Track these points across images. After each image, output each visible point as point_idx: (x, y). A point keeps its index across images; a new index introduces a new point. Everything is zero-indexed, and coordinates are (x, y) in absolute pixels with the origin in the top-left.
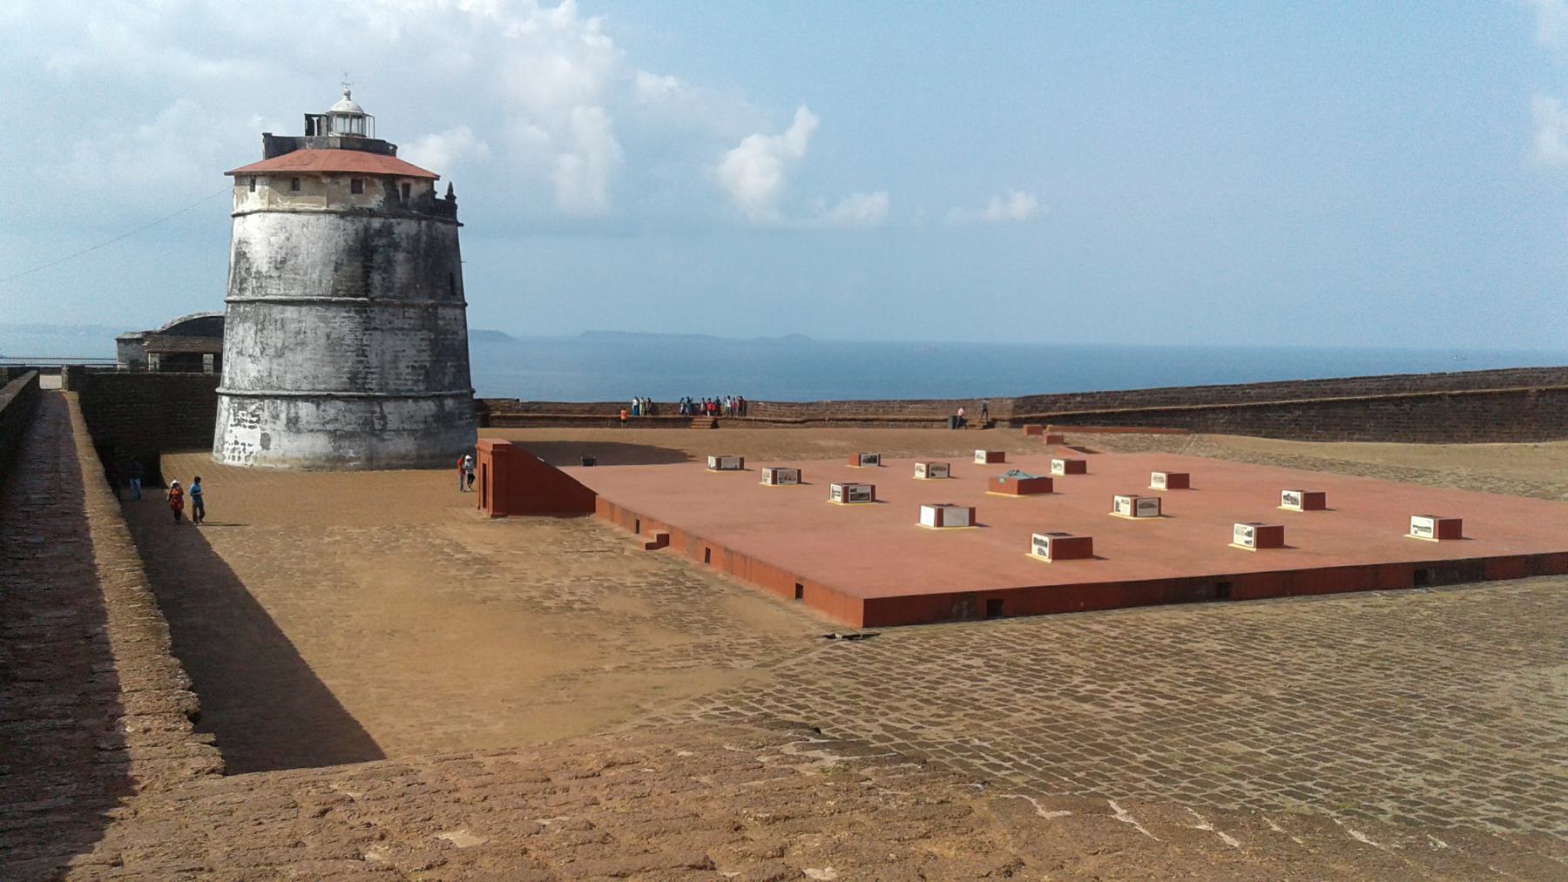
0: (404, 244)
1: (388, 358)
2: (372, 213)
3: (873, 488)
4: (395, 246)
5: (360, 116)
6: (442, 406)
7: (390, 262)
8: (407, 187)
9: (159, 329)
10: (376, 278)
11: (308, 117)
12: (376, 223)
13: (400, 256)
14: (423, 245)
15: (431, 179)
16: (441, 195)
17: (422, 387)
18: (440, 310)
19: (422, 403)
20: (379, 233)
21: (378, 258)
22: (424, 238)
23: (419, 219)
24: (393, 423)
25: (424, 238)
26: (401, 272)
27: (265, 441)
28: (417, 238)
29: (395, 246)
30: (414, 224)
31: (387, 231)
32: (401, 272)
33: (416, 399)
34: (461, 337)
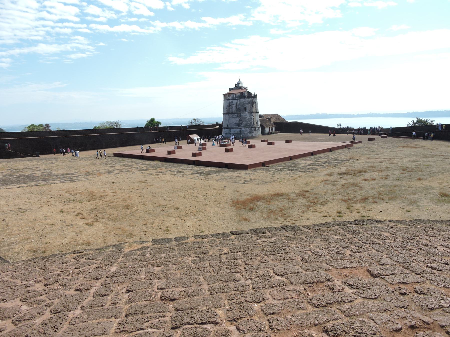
2: (230, 100)
4: (233, 104)
8: (235, 95)
10: (231, 110)
12: (231, 101)
29: (233, 104)
32: (234, 108)
33: (236, 128)
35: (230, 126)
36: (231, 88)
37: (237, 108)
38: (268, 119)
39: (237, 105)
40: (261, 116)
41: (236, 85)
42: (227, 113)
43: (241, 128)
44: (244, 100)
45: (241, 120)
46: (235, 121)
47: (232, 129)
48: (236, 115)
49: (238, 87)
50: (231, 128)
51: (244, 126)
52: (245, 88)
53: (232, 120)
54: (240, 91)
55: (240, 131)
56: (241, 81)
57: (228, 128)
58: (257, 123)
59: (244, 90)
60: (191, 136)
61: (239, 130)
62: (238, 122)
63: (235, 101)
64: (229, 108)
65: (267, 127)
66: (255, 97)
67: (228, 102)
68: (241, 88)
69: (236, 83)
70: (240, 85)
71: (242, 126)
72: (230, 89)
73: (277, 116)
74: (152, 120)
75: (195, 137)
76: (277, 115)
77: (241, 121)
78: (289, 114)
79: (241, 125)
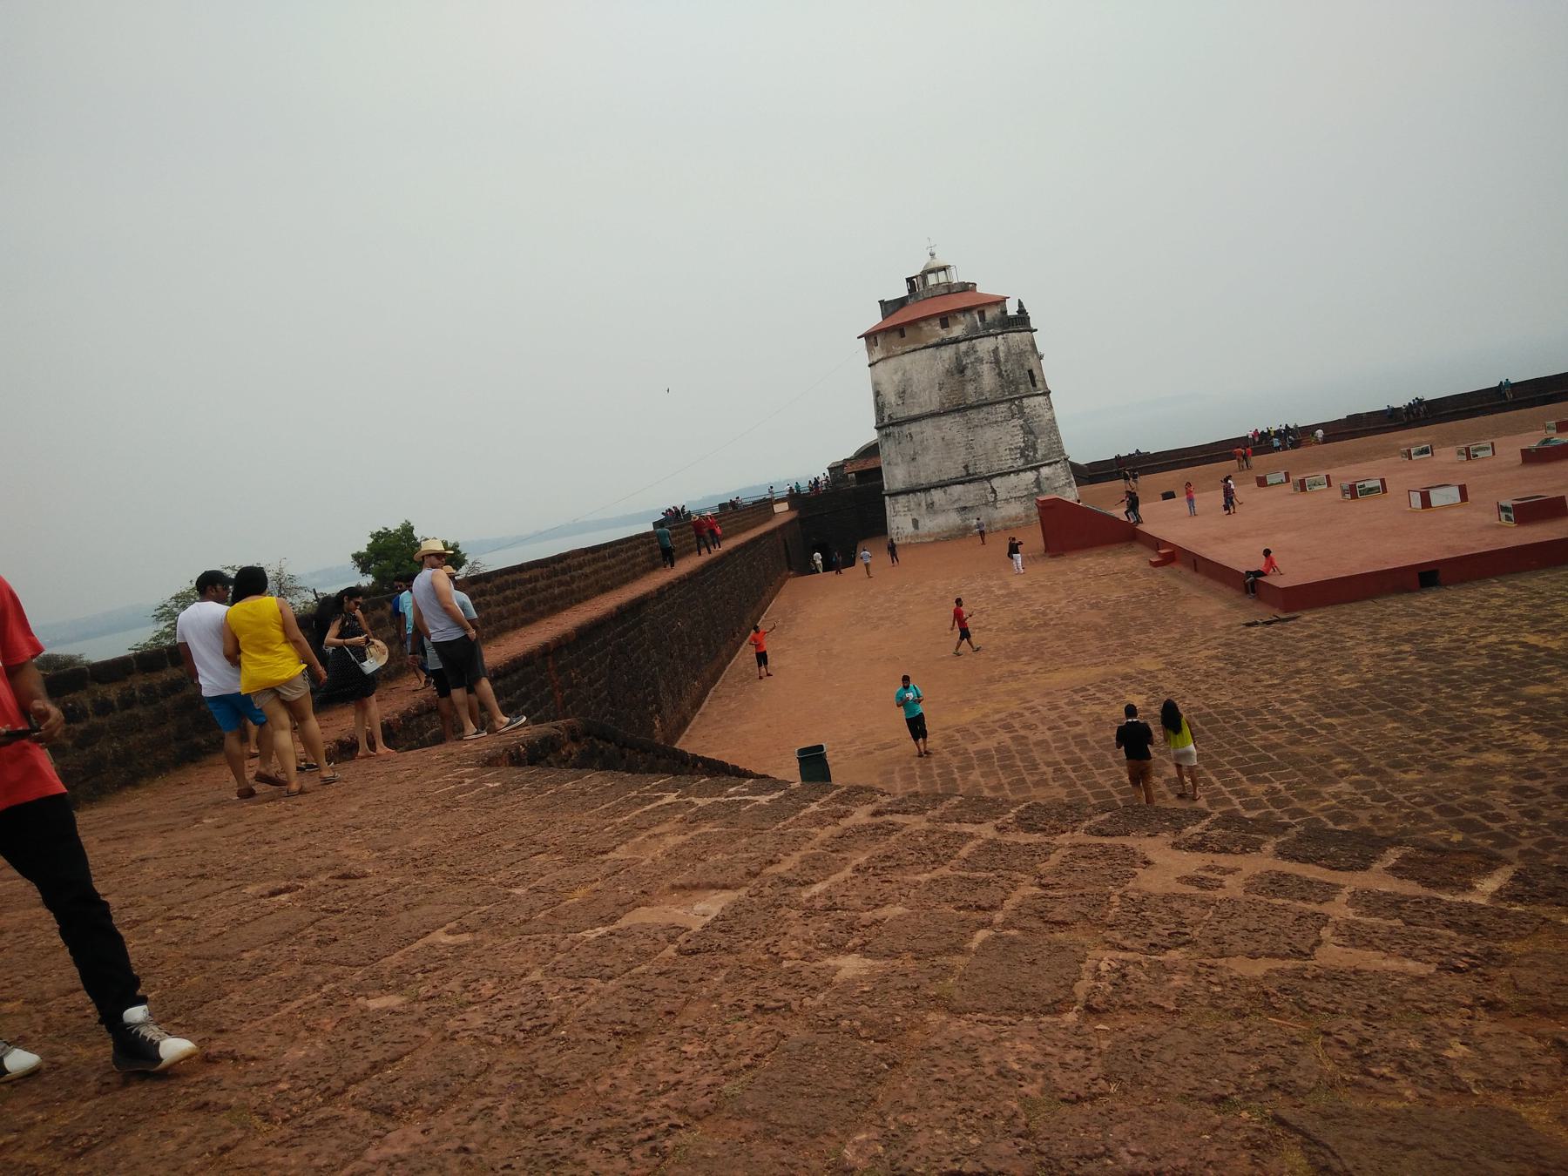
0: (986, 357)
2: (956, 341)
3: (1383, 481)
4: (980, 360)
5: (944, 269)
7: (979, 375)
9: (850, 454)
10: (970, 388)
11: (909, 280)
12: (963, 346)
15: (1001, 302)
16: (1012, 310)
17: (1021, 462)
20: (966, 354)
21: (969, 373)
24: (1001, 495)
25: (1002, 348)
27: (915, 523)
30: (992, 339)
32: (988, 379)
33: (1017, 472)
34: (1048, 416)
35: (982, 469)
37: (1000, 374)
39: (997, 362)
43: (1037, 468)
45: (1028, 431)
47: (996, 482)
48: (1003, 407)
50: (989, 478)
51: (1045, 456)
53: (989, 434)
55: (1038, 482)
61: (1030, 476)
62: (1019, 441)
63: (985, 346)
64: (962, 383)
67: (948, 353)
69: (916, 271)
71: (1039, 456)
77: (1032, 433)
79: (1035, 450)
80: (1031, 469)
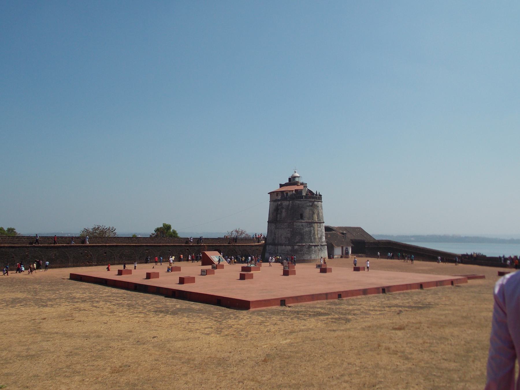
1: (280, 235)
4: (283, 208)
6: (293, 247)
7: (281, 212)
8: (287, 194)
10: (279, 216)
12: (279, 203)
13: (284, 210)
14: (290, 207)
17: (287, 242)
18: (295, 223)
19: (287, 247)
21: (279, 211)
22: (291, 205)
23: (289, 201)
25: (291, 205)
26: (284, 214)
28: (289, 205)
29: (283, 208)
30: (288, 202)
31: (281, 204)
33: (285, 246)
36: (283, 183)
38: (343, 234)
40: (328, 229)
41: (290, 179)
42: (275, 219)
44: (299, 202)
46: (284, 233)
47: (279, 247)
49: (292, 181)
52: (302, 184)
54: (294, 188)
56: (297, 175)
57: (274, 244)
58: (321, 238)
59: (301, 187)
60: (208, 253)
61: (289, 248)
63: (286, 203)
64: (277, 214)
65: (338, 246)
66: (319, 197)
67: (275, 204)
68: (296, 184)
69: (290, 176)
70: (297, 179)
72: (281, 186)
73: (359, 230)
74: (167, 227)
75: (215, 256)
76: (360, 228)
78: (380, 227)
80: (290, 245)
